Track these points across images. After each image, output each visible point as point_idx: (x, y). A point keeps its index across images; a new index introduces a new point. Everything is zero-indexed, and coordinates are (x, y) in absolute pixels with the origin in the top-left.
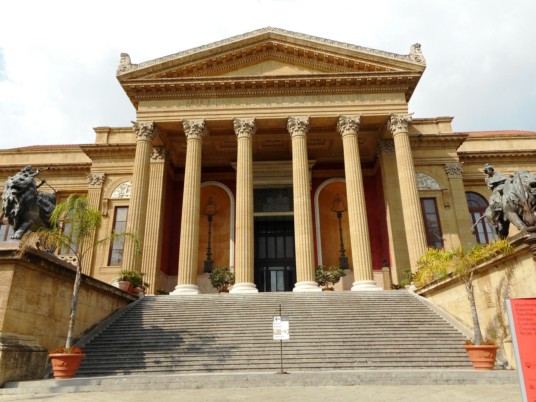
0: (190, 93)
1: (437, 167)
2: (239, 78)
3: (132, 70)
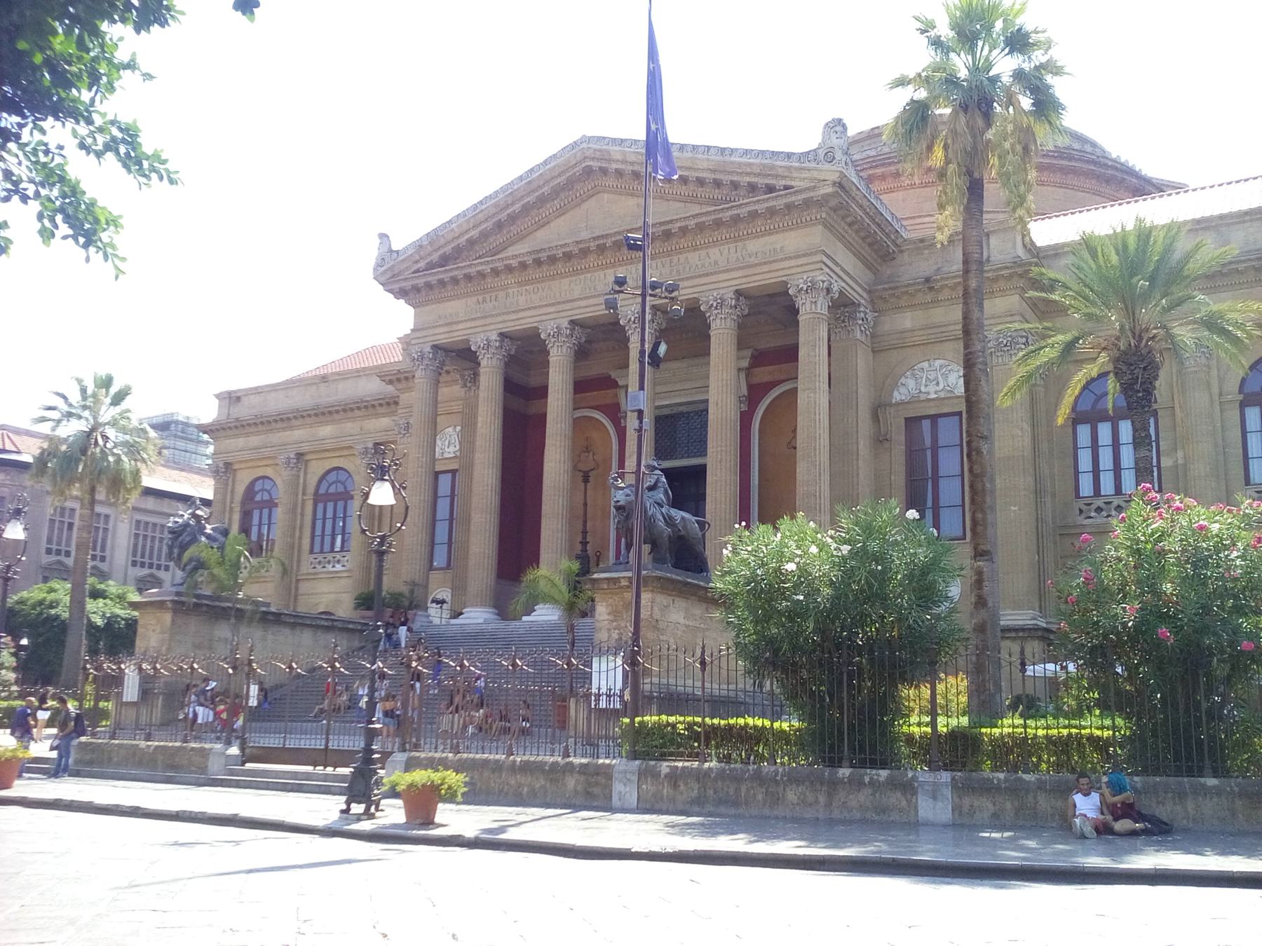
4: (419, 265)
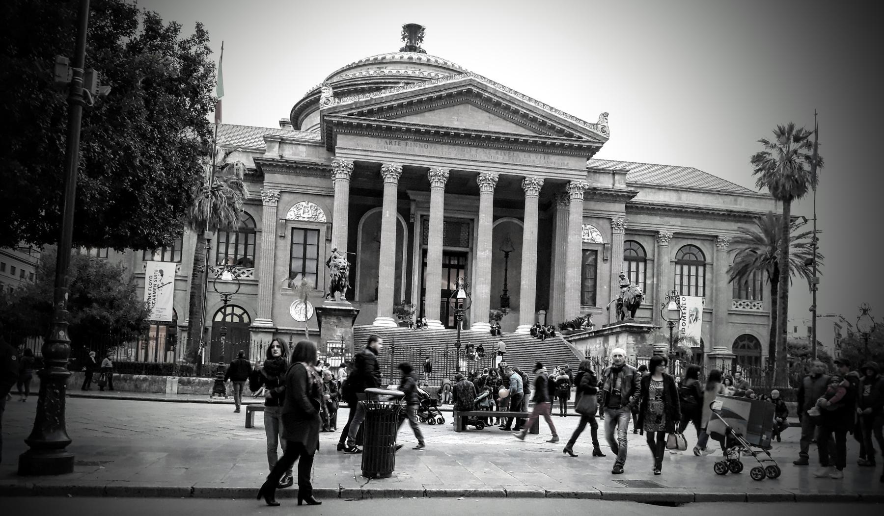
0: (390, 133)
1: (605, 221)
2: (438, 127)
3: (336, 105)
4: (353, 111)
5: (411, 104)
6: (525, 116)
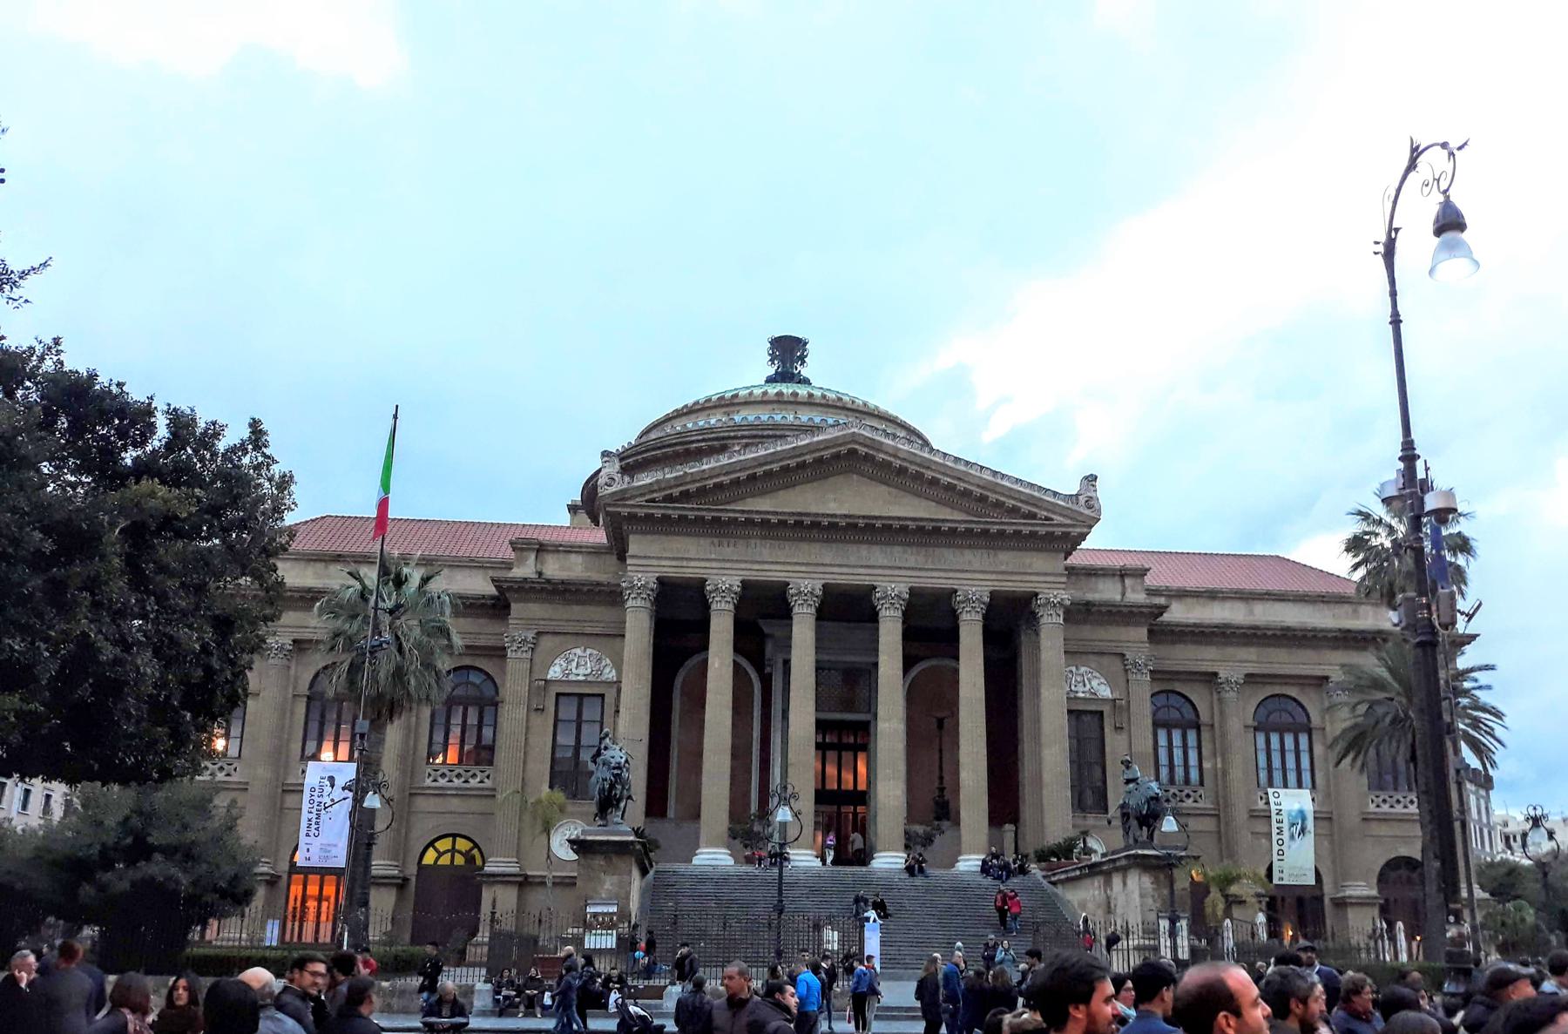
0: (719, 528)
5: (753, 478)
6: (950, 488)
